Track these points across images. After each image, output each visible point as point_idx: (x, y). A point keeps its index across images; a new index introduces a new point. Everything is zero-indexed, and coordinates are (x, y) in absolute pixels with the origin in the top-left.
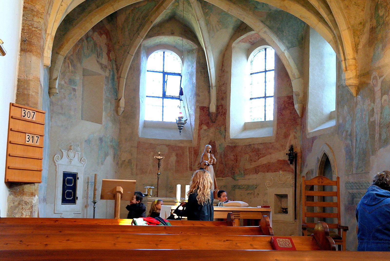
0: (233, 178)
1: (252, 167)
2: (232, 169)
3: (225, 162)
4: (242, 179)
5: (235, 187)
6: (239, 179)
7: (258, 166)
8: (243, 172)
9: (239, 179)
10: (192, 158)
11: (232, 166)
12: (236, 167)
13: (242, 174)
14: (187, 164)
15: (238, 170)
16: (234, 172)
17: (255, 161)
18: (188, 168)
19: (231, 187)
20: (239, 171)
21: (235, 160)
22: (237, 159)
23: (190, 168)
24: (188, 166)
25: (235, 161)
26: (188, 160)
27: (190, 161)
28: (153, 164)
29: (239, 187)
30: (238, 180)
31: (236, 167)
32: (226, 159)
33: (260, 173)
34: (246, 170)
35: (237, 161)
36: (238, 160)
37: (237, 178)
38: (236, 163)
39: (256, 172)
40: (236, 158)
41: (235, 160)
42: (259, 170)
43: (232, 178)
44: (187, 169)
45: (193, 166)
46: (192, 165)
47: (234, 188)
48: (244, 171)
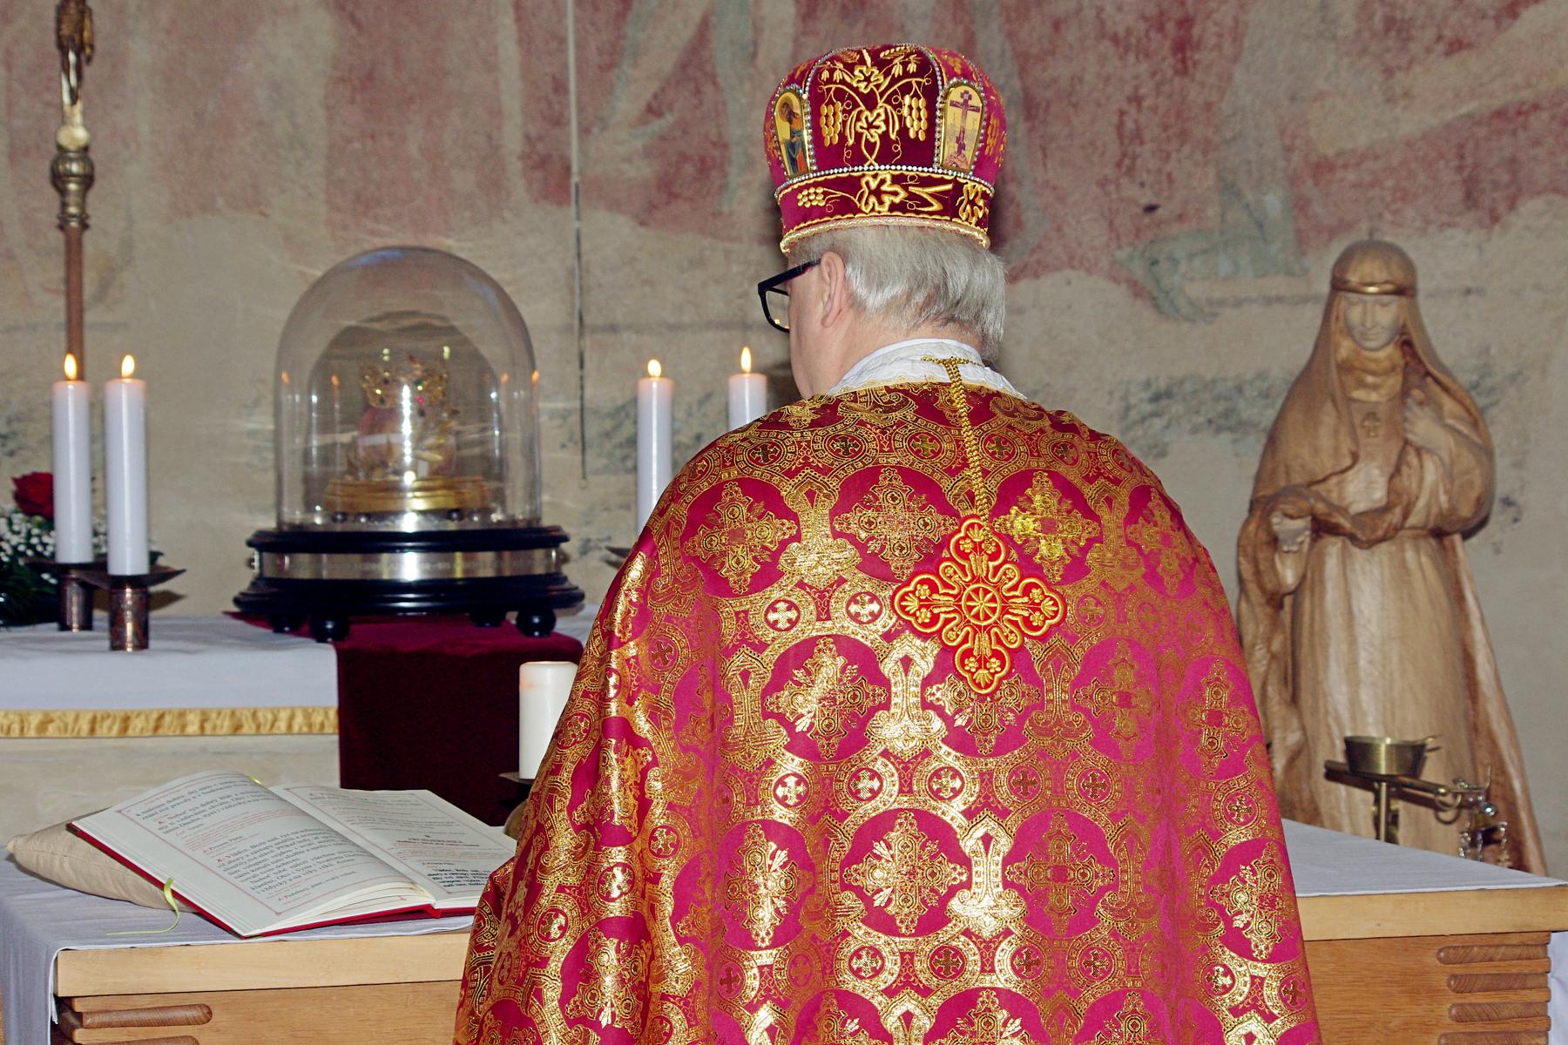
0: (1137, 290)
1: (1412, 122)
2: (1127, 165)
3: (1024, 60)
4: (1269, 301)
5: (1177, 408)
6: (1222, 303)
7: (1500, 114)
8: (1274, 202)
9: (1218, 293)
10: (561, 15)
11: (1122, 113)
12: (1184, 135)
13: (1260, 225)
14: (496, 113)
15: (1211, 172)
16: (1151, 209)
17: (1457, 46)
18: (515, 166)
19: (1116, 406)
20: (1228, 188)
21: (1161, 28)
22: (1186, 23)
23: (543, 163)
24: (512, 139)
25: (1162, 46)
26: (509, 51)
27: (526, 71)
28: (18, 123)
29: (1227, 414)
30: (1208, 311)
31: (1184, 135)
32: (1034, 30)
33: (1531, 207)
34: (1322, 168)
35: (1182, 47)
36: (1204, 30)
37: (1196, 290)
38: (1183, 69)
39: (1471, 198)
40: (1177, 13)
41: (1161, 28)
42: (1512, 163)
43: (1118, 293)
44: (494, 185)
45: (585, 131)
46: (558, 121)
47: (1158, 423)
48: (1293, 180)
